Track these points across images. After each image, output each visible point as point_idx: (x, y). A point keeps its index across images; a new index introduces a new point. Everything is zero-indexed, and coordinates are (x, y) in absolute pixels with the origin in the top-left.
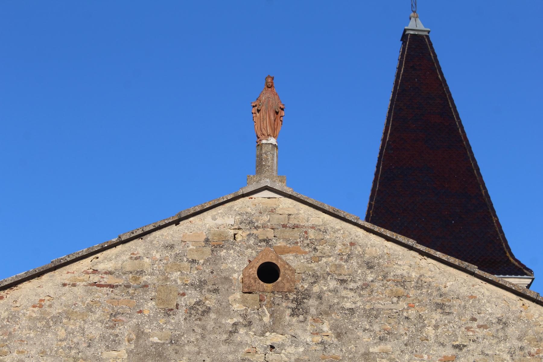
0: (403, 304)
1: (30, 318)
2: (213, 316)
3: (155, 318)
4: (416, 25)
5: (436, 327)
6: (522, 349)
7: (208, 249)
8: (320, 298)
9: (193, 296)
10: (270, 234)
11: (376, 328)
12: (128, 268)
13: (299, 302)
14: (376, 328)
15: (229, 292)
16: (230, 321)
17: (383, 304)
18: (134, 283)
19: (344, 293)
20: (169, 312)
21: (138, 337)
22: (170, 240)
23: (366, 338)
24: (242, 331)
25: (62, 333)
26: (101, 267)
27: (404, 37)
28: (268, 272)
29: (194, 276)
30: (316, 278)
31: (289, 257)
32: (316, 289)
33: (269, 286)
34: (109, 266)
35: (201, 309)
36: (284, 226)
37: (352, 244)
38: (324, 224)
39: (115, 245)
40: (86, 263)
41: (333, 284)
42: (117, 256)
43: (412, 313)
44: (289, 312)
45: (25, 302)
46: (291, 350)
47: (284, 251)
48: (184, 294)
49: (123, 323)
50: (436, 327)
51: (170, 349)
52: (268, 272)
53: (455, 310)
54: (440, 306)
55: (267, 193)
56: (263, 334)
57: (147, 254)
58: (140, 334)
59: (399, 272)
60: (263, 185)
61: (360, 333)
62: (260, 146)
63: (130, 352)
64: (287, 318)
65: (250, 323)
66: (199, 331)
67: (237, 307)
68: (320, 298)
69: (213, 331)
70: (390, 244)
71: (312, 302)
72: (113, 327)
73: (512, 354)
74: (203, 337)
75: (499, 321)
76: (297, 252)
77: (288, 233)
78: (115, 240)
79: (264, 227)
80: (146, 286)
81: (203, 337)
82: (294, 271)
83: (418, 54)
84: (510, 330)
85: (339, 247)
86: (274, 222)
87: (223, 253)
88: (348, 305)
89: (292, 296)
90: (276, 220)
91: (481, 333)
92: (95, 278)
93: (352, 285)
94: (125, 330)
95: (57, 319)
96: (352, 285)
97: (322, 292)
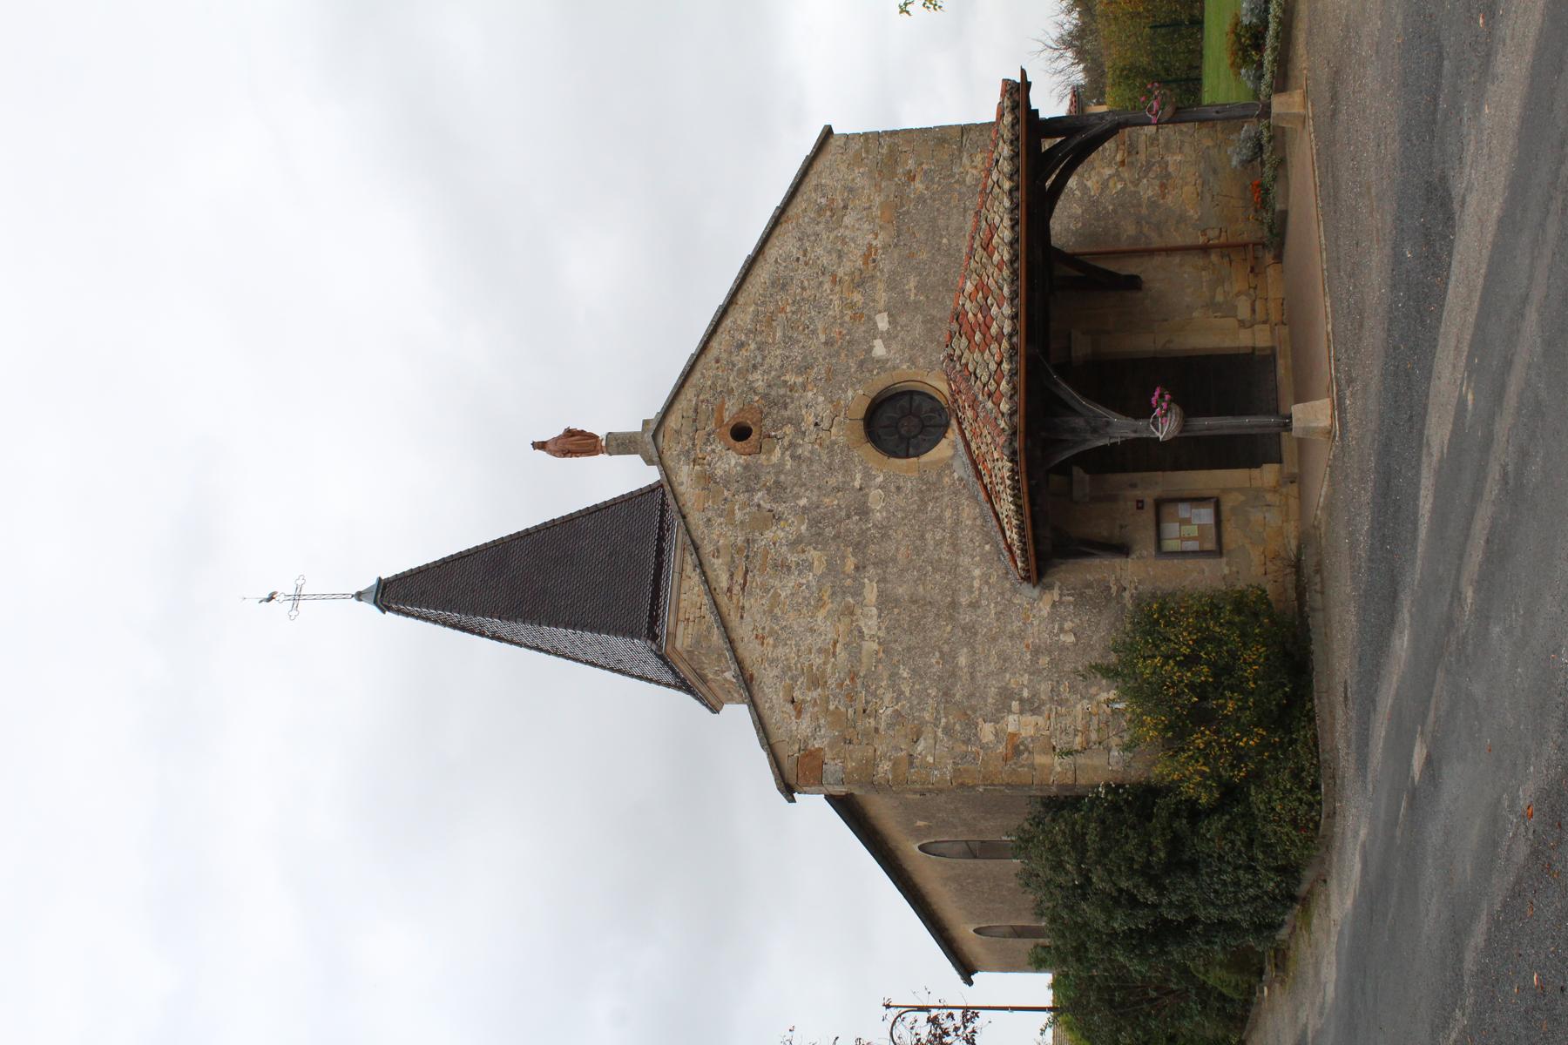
1: (775, 646)
2: (782, 477)
26: (724, 584)
31: (727, 417)
40: (723, 600)
41: (757, 375)
44: (783, 412)
50: (804, 289)
52: (740, 433)
72: (789, 568)
76: (721, 408)
77: (702, 417)
84: (809, 231)
87: (719, 472)
92: (737, 589)
96: (759, 359)
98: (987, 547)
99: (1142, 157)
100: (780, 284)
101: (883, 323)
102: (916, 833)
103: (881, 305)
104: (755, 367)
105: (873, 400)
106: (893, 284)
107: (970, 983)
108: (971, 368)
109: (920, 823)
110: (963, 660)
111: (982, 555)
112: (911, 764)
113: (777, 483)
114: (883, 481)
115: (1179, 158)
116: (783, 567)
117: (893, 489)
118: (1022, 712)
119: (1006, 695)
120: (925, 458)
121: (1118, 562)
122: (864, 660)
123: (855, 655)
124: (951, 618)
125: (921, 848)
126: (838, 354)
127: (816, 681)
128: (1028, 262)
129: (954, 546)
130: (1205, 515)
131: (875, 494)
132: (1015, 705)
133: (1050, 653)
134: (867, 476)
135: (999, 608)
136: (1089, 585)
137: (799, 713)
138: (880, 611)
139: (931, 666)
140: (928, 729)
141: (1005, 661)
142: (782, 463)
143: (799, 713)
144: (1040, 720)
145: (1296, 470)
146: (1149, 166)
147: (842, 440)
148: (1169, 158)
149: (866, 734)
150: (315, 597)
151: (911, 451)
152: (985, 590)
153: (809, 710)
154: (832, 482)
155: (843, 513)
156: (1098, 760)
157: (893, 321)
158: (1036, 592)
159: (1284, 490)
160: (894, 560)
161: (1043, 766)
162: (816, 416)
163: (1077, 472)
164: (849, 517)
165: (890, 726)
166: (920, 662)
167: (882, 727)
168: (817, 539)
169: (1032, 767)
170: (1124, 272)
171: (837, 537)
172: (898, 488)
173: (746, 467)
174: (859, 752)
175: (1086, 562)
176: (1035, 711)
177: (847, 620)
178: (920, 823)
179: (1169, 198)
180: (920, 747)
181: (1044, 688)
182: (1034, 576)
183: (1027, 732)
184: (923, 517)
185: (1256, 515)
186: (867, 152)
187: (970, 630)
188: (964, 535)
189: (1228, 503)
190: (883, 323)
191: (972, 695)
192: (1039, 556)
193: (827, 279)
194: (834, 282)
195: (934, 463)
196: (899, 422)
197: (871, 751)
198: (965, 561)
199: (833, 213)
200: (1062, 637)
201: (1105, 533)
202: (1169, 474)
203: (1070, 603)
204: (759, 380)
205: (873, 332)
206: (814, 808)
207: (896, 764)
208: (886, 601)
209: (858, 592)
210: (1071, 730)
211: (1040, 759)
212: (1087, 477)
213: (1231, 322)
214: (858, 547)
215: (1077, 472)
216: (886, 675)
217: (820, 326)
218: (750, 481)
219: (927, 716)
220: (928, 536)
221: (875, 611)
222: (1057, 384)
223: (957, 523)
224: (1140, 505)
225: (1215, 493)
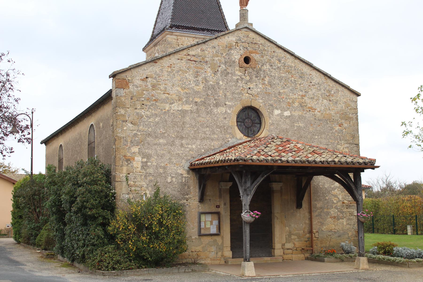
1: (167, 71)
2: (230, 75)
12: (200, 55)
28: (247, 60)
36: (252, 43)
40: (185, 52)
44: (254, 76)
48: (220, 66)
50: (300, 84)
52: (247, 60)
58: (207, 81)
60: (245, 26)
64: (254, 78)
66: (226, 80)
77: (253, 46)
80: (207, 62)
81: (227, 83)
84: (322, 87)
86: (248, 41)
90: (249, 40)
92: (189, 57)
96: (274, 67)
98: (203, 151)
99: (345, 210)
100: (302, 76)
101: (287, 113)
102: (98, 123)
104: (271, 66)
105: (258, 110)
106: (301, 118)
107: (42, 143)
108: (269, 145)
109: (101, 124)
110: (161, 141)
111: (200, 149)
112: (123, 121)
113: (228, 73)
114: (230, 112)
115: (345, 223)
116: (197, 75)
117: (225, 116)
118: (142, 162)
119: (149, 157)
120: (236, 128)
121: (197, 198)
122: (162, 104)
124: (177, 137)
125: (92, 125)
127: (154, 86)
128: (308, 167)
129: (204, 138)
130: (214, 230)
132: (145, 160)
133: (164, 173)
134: (230, 107)
135: (181, 155)
136: (189, 187)
137: (143, 80)
139: (159, 129)
140: (136, 128)
141: (161, 156)
142: (235, 75)
143: (143, 80)
144: (139, 169)
145: (230, 263)
146: (342, 212)
147: (244, 97)
148: (345, 220)
149: (135, 105)
151: (239, 123)
152: (188, 150)
153: (143, 84)
154: (228, 94)
155: (216, 98)
156: (124, 190)
157: (287, 117)
158: (186, 168)
159: (222, 259)
160: (199, 116)
161: (122, 170)
162: (253, 88)
163: (230, 184)
165: (138, 114)
166: (161, 125)
167: (137, 111)
168: (207, 88)
169: (122, 166)
170: (303, 202)
171: (208, 95)
172: (225, 118)
173: (234, 62)
174: (128, 102)
175: (197, 187)
176: (143, 167)
177: (177, 98)
178: (101, 124)
179: (330, 220)
180: (130, 125)
181: (151, 171)
182: (193, 167)
183: (135, 164)
184: (215, 127)
185: (213, 249)
186: (350, 109)
187: (173, 144)
188: (208, 142)
189: (218, 238)
190: (287, 113)
191: (149, 144)
192: (200, 169)
193: (304, 93)
194: (302, 96)
195: (235, 132)
196: (250, 119)
197: (128, 107)
198: (198, 142)
199: (328, 96)
201: (207, 194)
202: (229, 217)
203: (182, 180)
204: (267, 67)
205: (283, 110)
206: (107, 85)
207: (123, 116)
208: (184, 113)
209: (187, 102)
210: (135, 180)
211: (125, 169)
212: (228, 187)
213: (284, 241)
215: (230, 184)
216: (157, 112)
218: (230, 63)
219: (141, 127)
220: (208, 129)
221: (180, 109)
222: (262, 177)
223: (212, 140)
224: (218, 207)
225: (222, 234)
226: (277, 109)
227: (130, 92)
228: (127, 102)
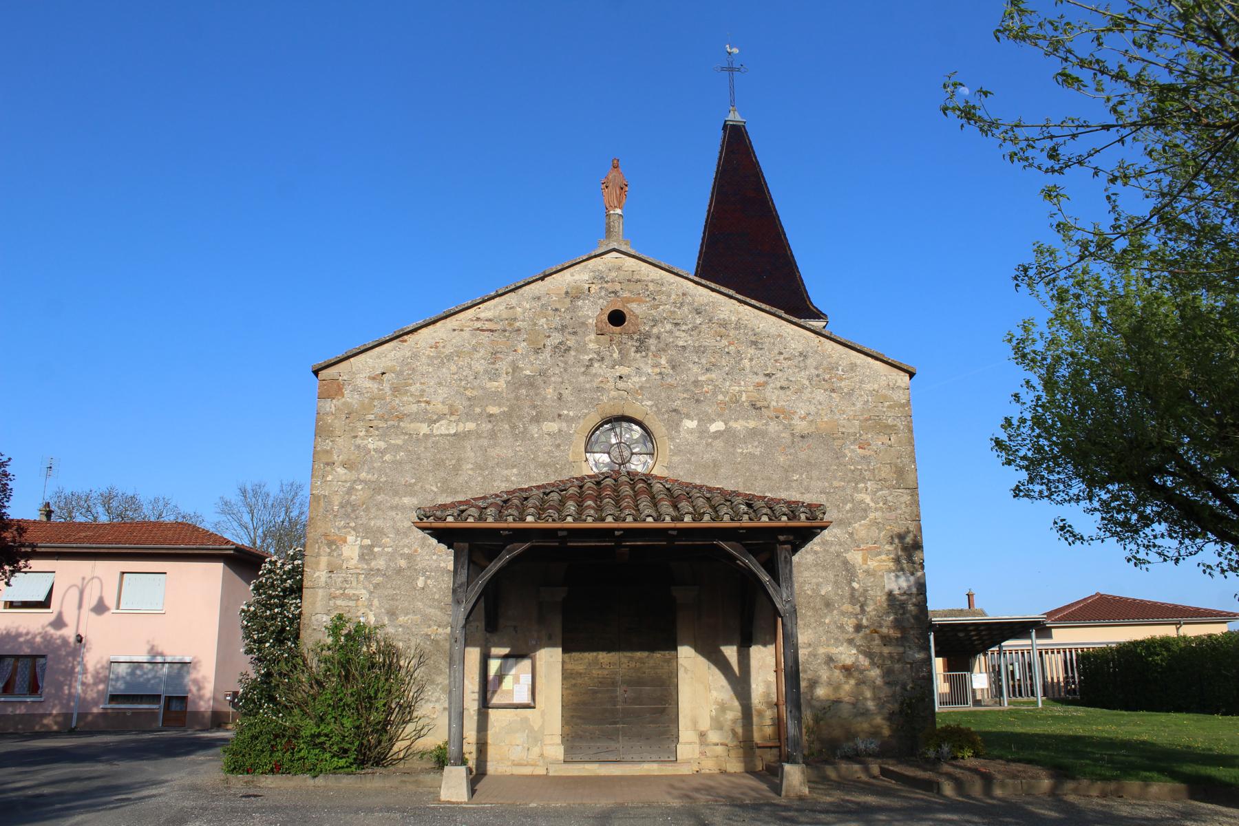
0: (725, 342)
1: (429, 356)
2: (573, 353)
3: (527, 355)
4: (734, 117)
5: (751, 360)
6: (818, 376)
7: (568, 300)
8: (658, 338)
9: (556, 338)
10: (618, 287)
11: (704, 361)
12: (504, 316)
13: (641, 341)
14: (704, 361)
15: (585, 335)
16: (587, 357)
17: (709, 342)
18: (509, 328)
19: (678, 334)
20: (537, 351)
21: (514, 371)
22: (537, 293)
23: (695, 369)
24: (596, 365)
25: (454, 368)
26: (482, 315)
27: (725, 127)
28: (617, 318)
29: (557, 321)
30: (655, 322)
32: (655, 330)
33: (618, 329)
34: (489, 314)
35: (563, 348)
37: (684, 294)
38: (662, 279)
39: (493, 298)
41: (669, 327)
42: (495, 306)
43: (732, 348)
44: (633, 349)
45: (424, 344)
46: (636, 379)
47: (629, 300)
49: (502, 360)
50: (751, 360)
51: (539, 380)
52: (617, 318)
53: (766, 346)
54: (754, 343)
55: (614, 254)
56: (613, 367)
57: (519, 305)
58: (515, 368)
59: (722, 316)
61: (691, 366)
62: (608, 216)
63: (508, 383)
65: (603, 359)
67: (592, 346)
68: (658, 338)
69: (573, 365)
70: (714, 294)
71: (652, 341)
72: (493, 363)
73: (810, 380)
74: (565, 370)
75: (801, 354)
76: (640, 301)
77: (632, 286)
78: (493, 294)
79: (613, 281)
81: (565, 370)
82: (637, 317)
83: (736, 143)
84: (809, 361)
85: (673, 296)
86: (621, 278)
87: (580, 303)
88: (681, 343)
89: (636, 336)
90: (622, 275)
91: (786, 364)
92: (478, 325)
93: (684, 327)
94: (503, 365)
95: (449, 358)
96: (684, 327)
97: (660, 333)
101: (717, 426)
103: (733, 424)
106: (753, 433)
110: (406, 500)
112: (328, 464)
116: (495, 356)
118: (362, 547)
119: (376, 534)
121: (482, 625)
123: (415, 418)
126: (687, 391)
127: (396, 390)
128: (614, 530)
130: (525, 698)
131: (553, 427)
132: (367, 542)
134: (569, 420)
138: (455, 435)
140: (353, 475)
142: (585, 352)
143: (374, 378)
144: (354, 562)
147: (605, 399)
150: (732, 81)
153: (374, 386)
154: (566, 393)
156: (319, 606)
157: (718, 435)
161: (318, 563)
162: (629, 376)
164: (535, 407)
167: (358, 441)
168: (515, 385)
169: (318, 555)
171: (517, 398)
172: (559, 446)
174: (338, 424)
176: (362, 557)
177: (446, 411)
180: (341, 470)
181: (380, 563)
184: (532, 467)
185: (520, 738)
193: (762, 379)
194: (758, 385)
197: (338, 433)
199: (827, 379)
200: (422, 579)
209: (469, 416)
211: (324, 560)
214: (508, 416)
217: (713, 376)
218: (574, 328)
221: (453, 432)
226: (688, 416)
227: (344, 404)
228: (337, 423)
